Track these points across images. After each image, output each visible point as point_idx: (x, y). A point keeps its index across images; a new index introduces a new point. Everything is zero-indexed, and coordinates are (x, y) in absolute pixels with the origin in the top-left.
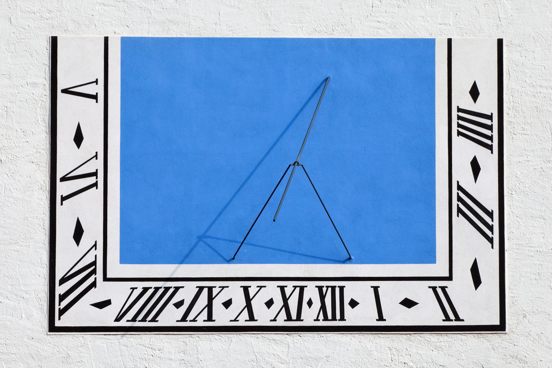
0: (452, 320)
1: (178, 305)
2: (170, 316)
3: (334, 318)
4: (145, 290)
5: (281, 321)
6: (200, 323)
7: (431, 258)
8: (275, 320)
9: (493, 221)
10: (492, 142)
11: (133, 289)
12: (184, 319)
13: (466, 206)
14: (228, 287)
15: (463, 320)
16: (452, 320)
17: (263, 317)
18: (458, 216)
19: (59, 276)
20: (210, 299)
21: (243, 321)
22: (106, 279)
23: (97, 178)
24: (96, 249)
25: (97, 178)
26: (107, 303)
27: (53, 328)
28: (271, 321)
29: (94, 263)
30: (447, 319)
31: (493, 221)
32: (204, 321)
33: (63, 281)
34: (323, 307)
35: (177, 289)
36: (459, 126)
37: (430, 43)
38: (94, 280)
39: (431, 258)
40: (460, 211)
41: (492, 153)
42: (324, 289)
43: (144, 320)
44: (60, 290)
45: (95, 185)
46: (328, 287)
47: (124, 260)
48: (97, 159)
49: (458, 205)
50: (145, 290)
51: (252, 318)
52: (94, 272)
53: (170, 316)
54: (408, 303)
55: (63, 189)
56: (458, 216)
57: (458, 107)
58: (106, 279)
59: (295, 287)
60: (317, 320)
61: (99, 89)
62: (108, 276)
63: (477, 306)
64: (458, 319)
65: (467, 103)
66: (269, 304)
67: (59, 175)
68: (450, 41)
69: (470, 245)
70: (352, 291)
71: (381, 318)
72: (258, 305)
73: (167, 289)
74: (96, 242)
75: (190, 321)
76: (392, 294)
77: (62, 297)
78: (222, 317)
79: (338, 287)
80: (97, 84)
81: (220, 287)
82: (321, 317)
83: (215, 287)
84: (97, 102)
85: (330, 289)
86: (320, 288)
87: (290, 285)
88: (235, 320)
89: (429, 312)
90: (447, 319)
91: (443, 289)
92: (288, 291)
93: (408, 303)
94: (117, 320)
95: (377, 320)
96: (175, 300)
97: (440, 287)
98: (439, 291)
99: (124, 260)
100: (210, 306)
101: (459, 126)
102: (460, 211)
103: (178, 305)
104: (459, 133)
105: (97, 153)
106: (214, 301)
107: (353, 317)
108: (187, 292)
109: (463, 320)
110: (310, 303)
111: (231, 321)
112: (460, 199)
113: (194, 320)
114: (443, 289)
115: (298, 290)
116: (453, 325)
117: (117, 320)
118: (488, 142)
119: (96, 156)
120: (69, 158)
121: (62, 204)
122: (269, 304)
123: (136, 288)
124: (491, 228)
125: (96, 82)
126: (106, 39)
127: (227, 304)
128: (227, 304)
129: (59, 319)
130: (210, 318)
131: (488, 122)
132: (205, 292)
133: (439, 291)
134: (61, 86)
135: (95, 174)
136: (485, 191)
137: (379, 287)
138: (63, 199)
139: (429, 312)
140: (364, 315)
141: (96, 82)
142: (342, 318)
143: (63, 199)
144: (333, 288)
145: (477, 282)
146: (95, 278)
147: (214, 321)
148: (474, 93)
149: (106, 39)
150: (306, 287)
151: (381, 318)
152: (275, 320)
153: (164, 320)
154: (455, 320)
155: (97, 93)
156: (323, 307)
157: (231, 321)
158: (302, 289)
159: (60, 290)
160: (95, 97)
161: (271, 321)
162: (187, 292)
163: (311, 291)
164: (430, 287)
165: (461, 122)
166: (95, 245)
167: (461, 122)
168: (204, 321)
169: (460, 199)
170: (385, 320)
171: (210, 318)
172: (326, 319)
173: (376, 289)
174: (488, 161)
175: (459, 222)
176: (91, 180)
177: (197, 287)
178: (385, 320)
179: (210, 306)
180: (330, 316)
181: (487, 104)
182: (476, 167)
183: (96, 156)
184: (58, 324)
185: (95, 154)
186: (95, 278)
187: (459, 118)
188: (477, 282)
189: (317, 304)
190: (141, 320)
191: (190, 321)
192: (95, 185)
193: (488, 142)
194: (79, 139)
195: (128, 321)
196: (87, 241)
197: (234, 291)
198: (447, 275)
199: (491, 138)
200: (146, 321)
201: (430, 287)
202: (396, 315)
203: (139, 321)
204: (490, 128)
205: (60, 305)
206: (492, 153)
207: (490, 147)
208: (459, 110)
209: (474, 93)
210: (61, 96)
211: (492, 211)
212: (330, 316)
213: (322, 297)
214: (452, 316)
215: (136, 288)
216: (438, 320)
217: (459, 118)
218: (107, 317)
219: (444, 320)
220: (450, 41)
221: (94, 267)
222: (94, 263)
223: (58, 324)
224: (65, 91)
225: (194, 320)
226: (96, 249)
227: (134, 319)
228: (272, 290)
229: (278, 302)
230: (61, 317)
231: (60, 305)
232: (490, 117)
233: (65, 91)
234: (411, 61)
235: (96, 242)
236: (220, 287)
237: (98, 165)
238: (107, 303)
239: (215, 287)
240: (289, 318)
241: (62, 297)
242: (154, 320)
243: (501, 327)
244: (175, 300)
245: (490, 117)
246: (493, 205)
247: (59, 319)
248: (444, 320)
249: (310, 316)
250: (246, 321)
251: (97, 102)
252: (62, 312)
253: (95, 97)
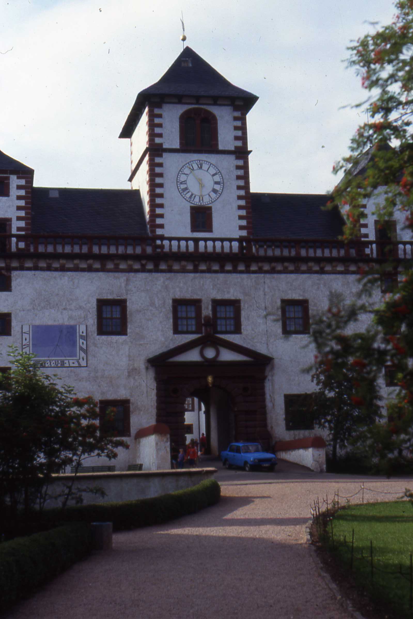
7: (76, 356)
13: (81, 349)
17: (53, 365)
39: (76, 356)
54: (73, 363)
63: (83, 363)
65: (81, 334)
69: (83, 355)
70: (65, 362)
72: (52, 363)
89: (76, 364)
93: (73, 363)
107: (65, 365)
120: (24, 342)
136: (84, 347)
139: (76, 364)
140: (67, 365)
145: (83, 360)
148: (83, 333)
163: (59, 362)
175: (81, 351)
181: (85, 334)
182: (83, 343)
188: (83, 360)
194: (26, 339)
197: (48, 362)
202: (72, 365)
209: (83, 333)
210: (23, 334)
228: (54, 362)
246: (85, 348)
249: (59, 365)
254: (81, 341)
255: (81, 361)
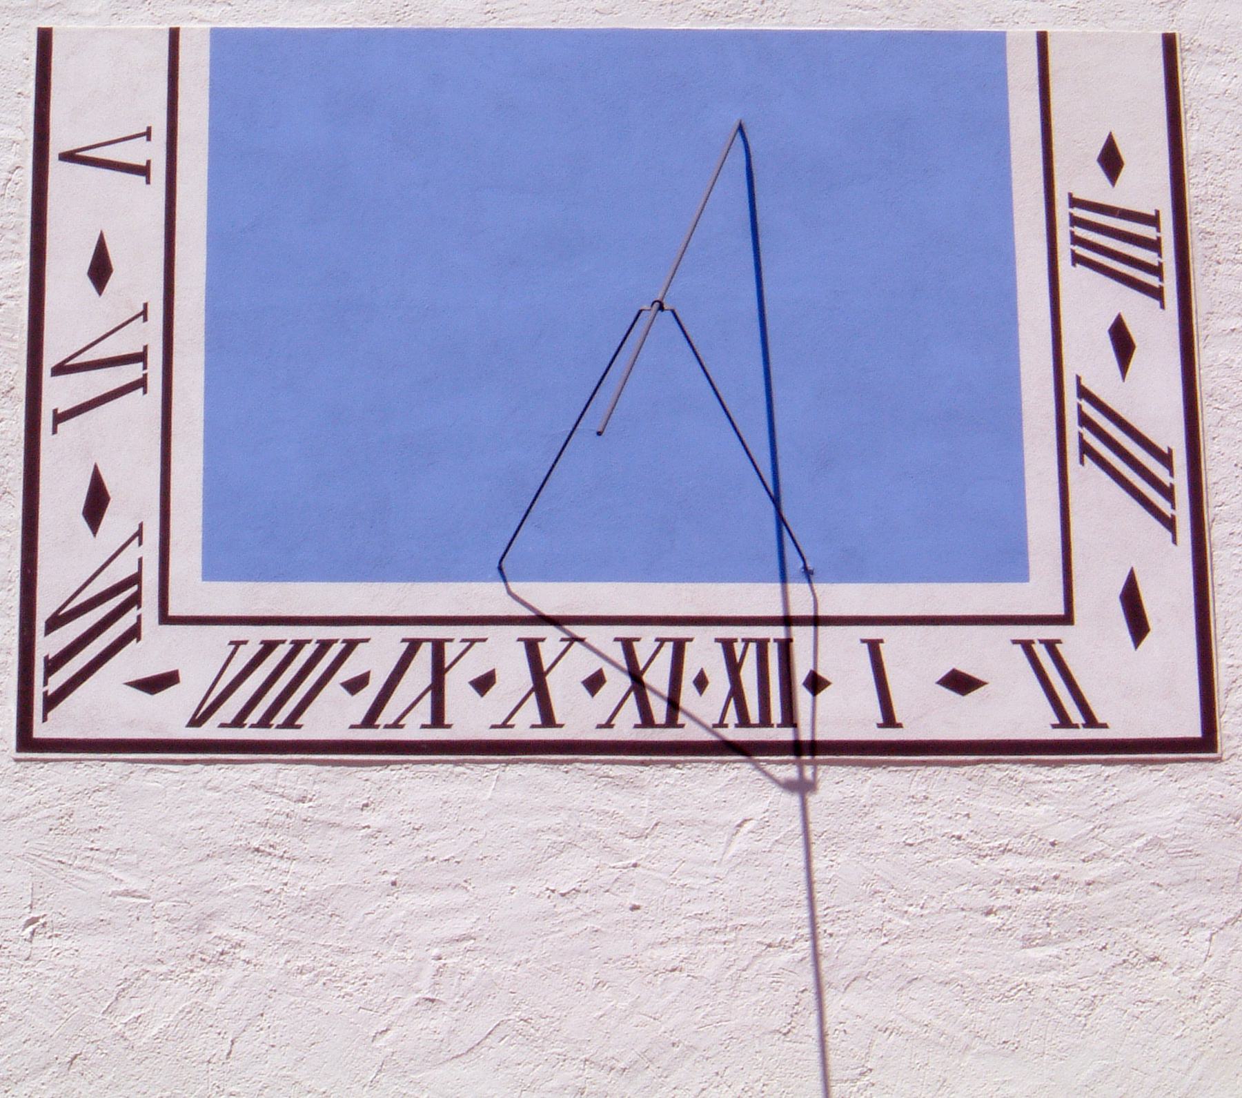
0: (1076, 726)
1: (356, 685)
2: (335, 714)
3: (765, 721)
4: (269, 647)
5: (627, 728)
6: (413, 731)
8: (609, 725)
9: (1172, 474)
10: (1161, 279)
11: (237, 644)
12: (370, 720)
13: (1101, 436)
14: (484, 640)
15: (1104, 726)
16: (1076, 726)
17: (579, 716)
18: (1082, 462)
19: (44, 610)
20: (439, 670)
21: (526, 726)
22: (165, 618)
23: (145, 368)
24: (140, 543)
25: (145, 368)
26: (167, 680)
27: (26, 741)
28: (600, 726)
29: (136, 579)
30: (1065, 722)
31: (1172, 474)
32: (424, 726)
33: (55, 622)
34: (736, 692)
35: (351, 645)
36: (1076, 240)
37: (995, 43)
38: (134, 621)
40: (1085, 449)
41: (1163, 307)
42: (738, 648)
43: (265, 723)
44: (47, 645)
45: (142, 383)
46: (747, 641)
47: (212, 571)
48: (145, 320)
49: (1081, 435)
50: (269, 647)
51: (548, 719)
52: (135, 600)
53: (335, 714)
54: (960, 683)
55: (59, 393)
56: (1082, 462)
57: (1070, 195)
58: (165, 618)
59: (662, 641)
60: (721, 724)
61: (155, 153)
62: (172, 612)
63: (1141, 688)
64: (1091, 721)
65: (1094, 186)
66: (594, 683)
67: (50, 359)
68: (1042, 39)
69: (1117, 535)
71: (889, 720)
72: (564, 685)
73: (325, 645)
74: (141, 526)
75: (387, 727)
76: (916, 660)
77: (53, 665)
78: (470, 717)
79: (775, 640)
80: (149, 139)
81: (464, 640)
82: (732, 717)
83: (451, 640)
84: (148, 182)
85: (752, 647)
86: (728, 645)
87: (646, 639)
88: (504, 725)
90: (1065, 722)
91: (1051, 646)
92: (642, 653)
93: (960, 683)
94: (196, 722)
95: (880, 726)
96: (348, 671)
97: (1041, 641)
98: (1041, 652)
99: (212, 571)
100: (437, 688)
101: (1076, 240)
102: (1085, 449)
103: (356, 685)
104: (1077, 259)
105: (146, 305)
106: (449, 677)
108: (378, 653)
109: (1104, 726)
110: (701, 682)
111: (494, 727)
112: (1084, 420)
113: (396, 725)
114: (1051, 646)
115: (668, 648)
116: (1079, 741)
117: (197, 721)
118: (1152, 280)
119: (144, 313)
121: (55, 431)
122: (594, 683)
123: (245, 642)
124: (1168, 493)
125: (148, 134)
126: (174, 35)
127: (484, 684)
128: (484, 684)
129: (45, 719)
130: (438, 719)
131: (1148, 232)
132: (426, 651)
133: (1041, 652)
134: (59, 142)
135: (141, 357)
137: (881, 641)
138: (59, 418)
141: (148, 134)
142: (789, 719)
143: (59, 418)
144: (762, 645)
145: (1138, 626)
146: (139, 618)
147: (449, 726)
148: (1111, 161)
149: (174, 35)
150: (691, 640)
151: (889, 720)
152: (609, 725)
153: (314, 727)
154: (1085, 726)
155: (149, 162)
156: (736, 692)
157: (494, 727)
158: (679, 646)
159: (47, 645)
160: (143, 171)
161: (600, 726)
162: (378, 653)
163: (704, 652)
164: (1015, 642)
165: (1081, 232)
166: (139, 534)
167: (1081, 232)
168: (424, 726)
169: (1084, 420)
170: (900, 726)
171: (438, 719)
172: (744, 721)
173: (874, 647)
174: (1154, 326)
176: (132, 372)
177: (404, 640)
178: (900, 726)
179: (437, 688)
180: (754, 715)
181: (1144, 186)
183: (144, 313)
184: (40, 731)
185: (141, 309)
186: (139, 618)
187: (1075, 221)
188: (1138, 626)
189: (720, 684)
190: (257, 726)
191: (387, 727)
192: (142, 383)
193: (1152, 280)
194: (100, 271)
195: (223, 725)
196: (116, 523)
197: (503, 652)
198: (1060, 610)
199: (1157, 271)
200: (269, 726)
201: (1015, 642)
202: (928, 714)
203: (252, 726)
204: (1155, 246)
205: (46, 683)
206: (1163, 307)
207: (1157, 294)
208: (1074, 202)
209: (1111, 161)
210: (56, 168)
211: (1170, 450)
212: (754, 715)
213: (734, 668)
214: (1075, 715)
215: (245, 642)
216: (1037, 722)
217: (1075, 221)
218: (168, 716)
219: (1054, 726)
220: (1042, 39)
221: (135, 588)
222: (136, 579)
223: (40, 731)
224: (70, 157)
225: (396, 725)
226: (140, 543)
227: (238, 722)
229: (618, 683)
230: (50, 715)
231: (46, 683)
232: (1153, 221)
233: (70, 157)
234: (947, 91)
235: (141, 526)
236: (464, 640)
237: (149, 335)
238: (167, 680)
239: (451, 640)
240: (647, 720)
241: (53, 665)
242: (290, 723)
243: (1205, 743)
244: (348, 671)
245: (1153, 221)
246: (1172, 438)
247: (45, 719)
248: (1054, 726)
250: (533, 726)
251: (148, 182)
252: (51, 702)
253: (143, 171)
254: (1093, 300)
255: (1094, 644)
